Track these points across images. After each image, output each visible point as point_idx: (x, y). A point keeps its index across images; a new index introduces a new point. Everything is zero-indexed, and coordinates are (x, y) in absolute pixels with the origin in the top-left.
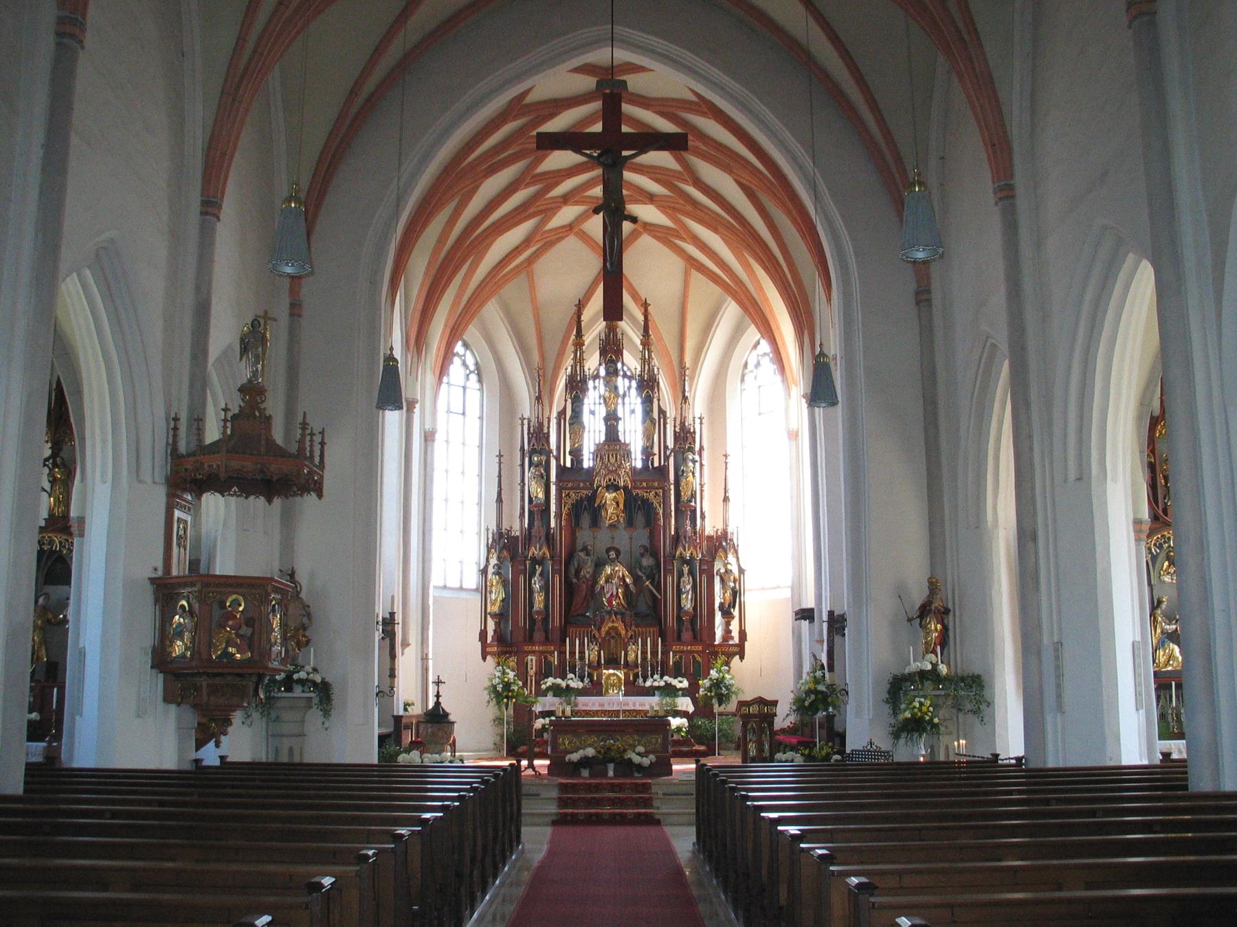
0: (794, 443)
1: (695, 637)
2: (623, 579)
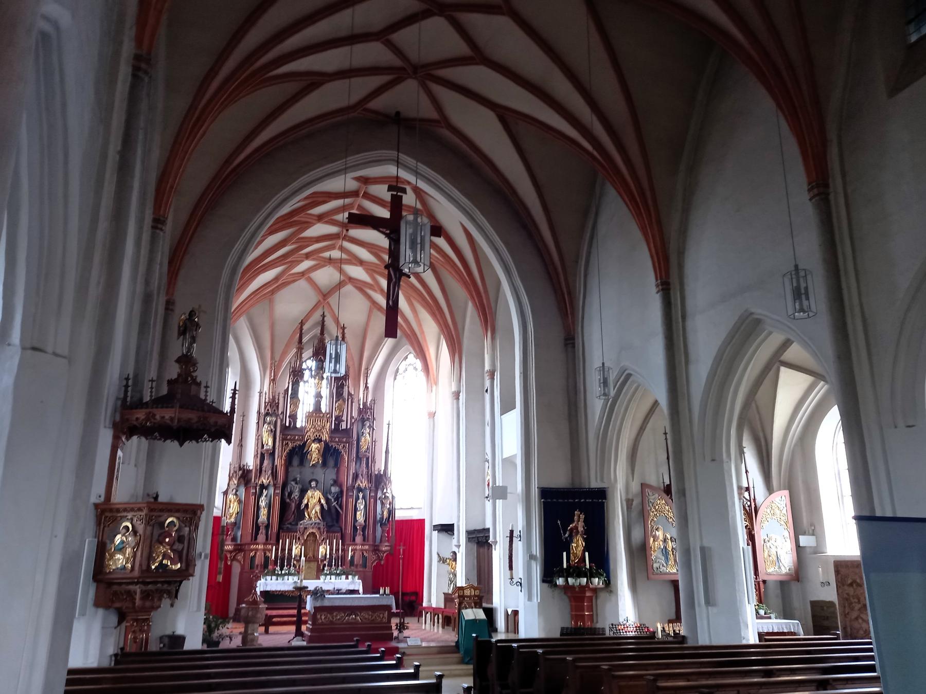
0: (432, 420)
1: (364, 540)
2: (319, 501)
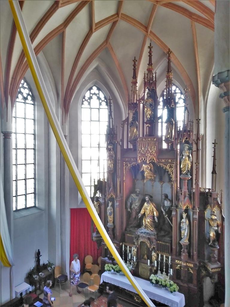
2: (153, 212)
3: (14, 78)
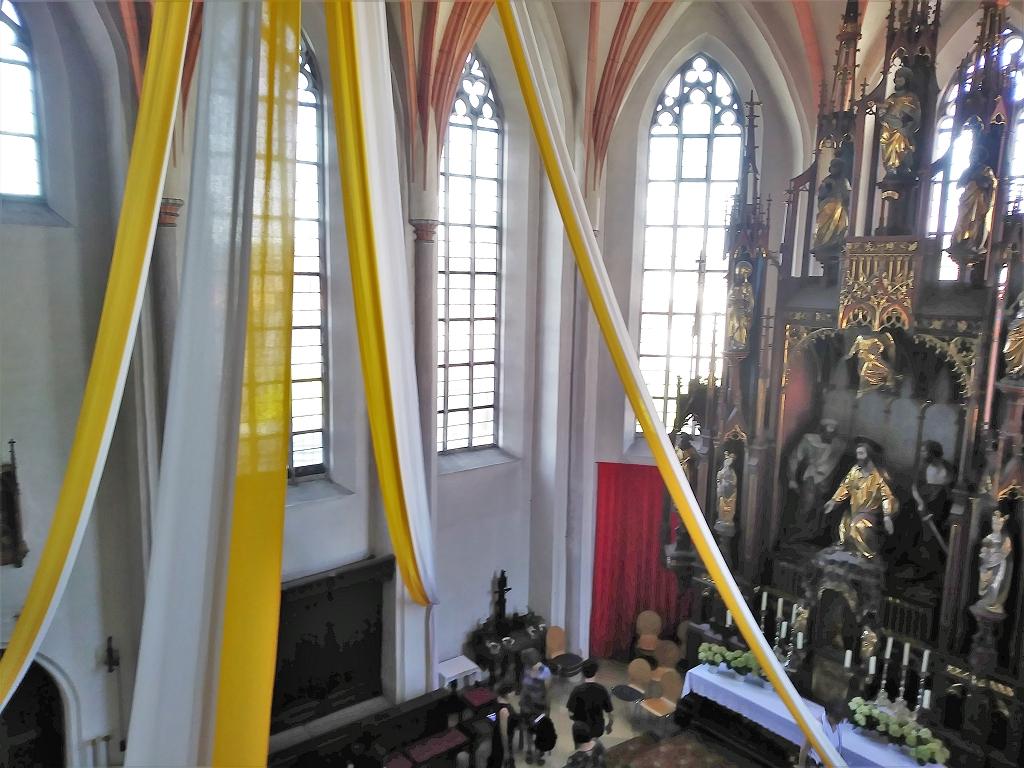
2: (879, 500)
3: (447, 49)
